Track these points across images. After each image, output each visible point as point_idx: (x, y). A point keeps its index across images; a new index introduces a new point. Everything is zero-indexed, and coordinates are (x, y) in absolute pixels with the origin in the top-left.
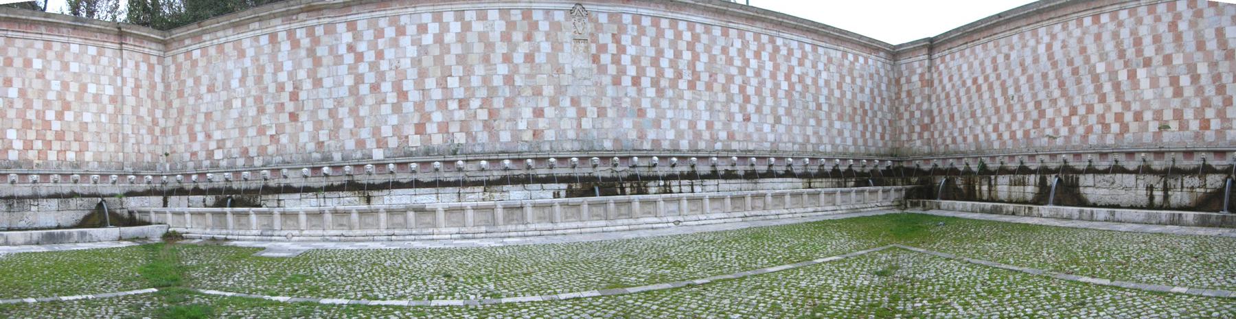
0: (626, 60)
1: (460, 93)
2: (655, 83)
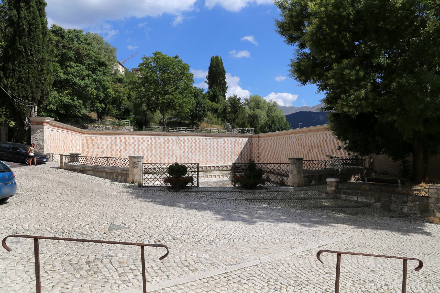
0: (186, 147)
1: (155, 154)
2: (191, 152)
